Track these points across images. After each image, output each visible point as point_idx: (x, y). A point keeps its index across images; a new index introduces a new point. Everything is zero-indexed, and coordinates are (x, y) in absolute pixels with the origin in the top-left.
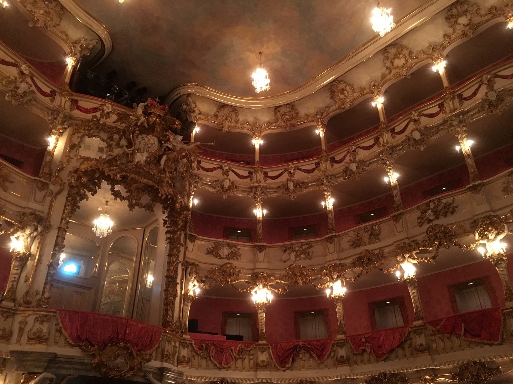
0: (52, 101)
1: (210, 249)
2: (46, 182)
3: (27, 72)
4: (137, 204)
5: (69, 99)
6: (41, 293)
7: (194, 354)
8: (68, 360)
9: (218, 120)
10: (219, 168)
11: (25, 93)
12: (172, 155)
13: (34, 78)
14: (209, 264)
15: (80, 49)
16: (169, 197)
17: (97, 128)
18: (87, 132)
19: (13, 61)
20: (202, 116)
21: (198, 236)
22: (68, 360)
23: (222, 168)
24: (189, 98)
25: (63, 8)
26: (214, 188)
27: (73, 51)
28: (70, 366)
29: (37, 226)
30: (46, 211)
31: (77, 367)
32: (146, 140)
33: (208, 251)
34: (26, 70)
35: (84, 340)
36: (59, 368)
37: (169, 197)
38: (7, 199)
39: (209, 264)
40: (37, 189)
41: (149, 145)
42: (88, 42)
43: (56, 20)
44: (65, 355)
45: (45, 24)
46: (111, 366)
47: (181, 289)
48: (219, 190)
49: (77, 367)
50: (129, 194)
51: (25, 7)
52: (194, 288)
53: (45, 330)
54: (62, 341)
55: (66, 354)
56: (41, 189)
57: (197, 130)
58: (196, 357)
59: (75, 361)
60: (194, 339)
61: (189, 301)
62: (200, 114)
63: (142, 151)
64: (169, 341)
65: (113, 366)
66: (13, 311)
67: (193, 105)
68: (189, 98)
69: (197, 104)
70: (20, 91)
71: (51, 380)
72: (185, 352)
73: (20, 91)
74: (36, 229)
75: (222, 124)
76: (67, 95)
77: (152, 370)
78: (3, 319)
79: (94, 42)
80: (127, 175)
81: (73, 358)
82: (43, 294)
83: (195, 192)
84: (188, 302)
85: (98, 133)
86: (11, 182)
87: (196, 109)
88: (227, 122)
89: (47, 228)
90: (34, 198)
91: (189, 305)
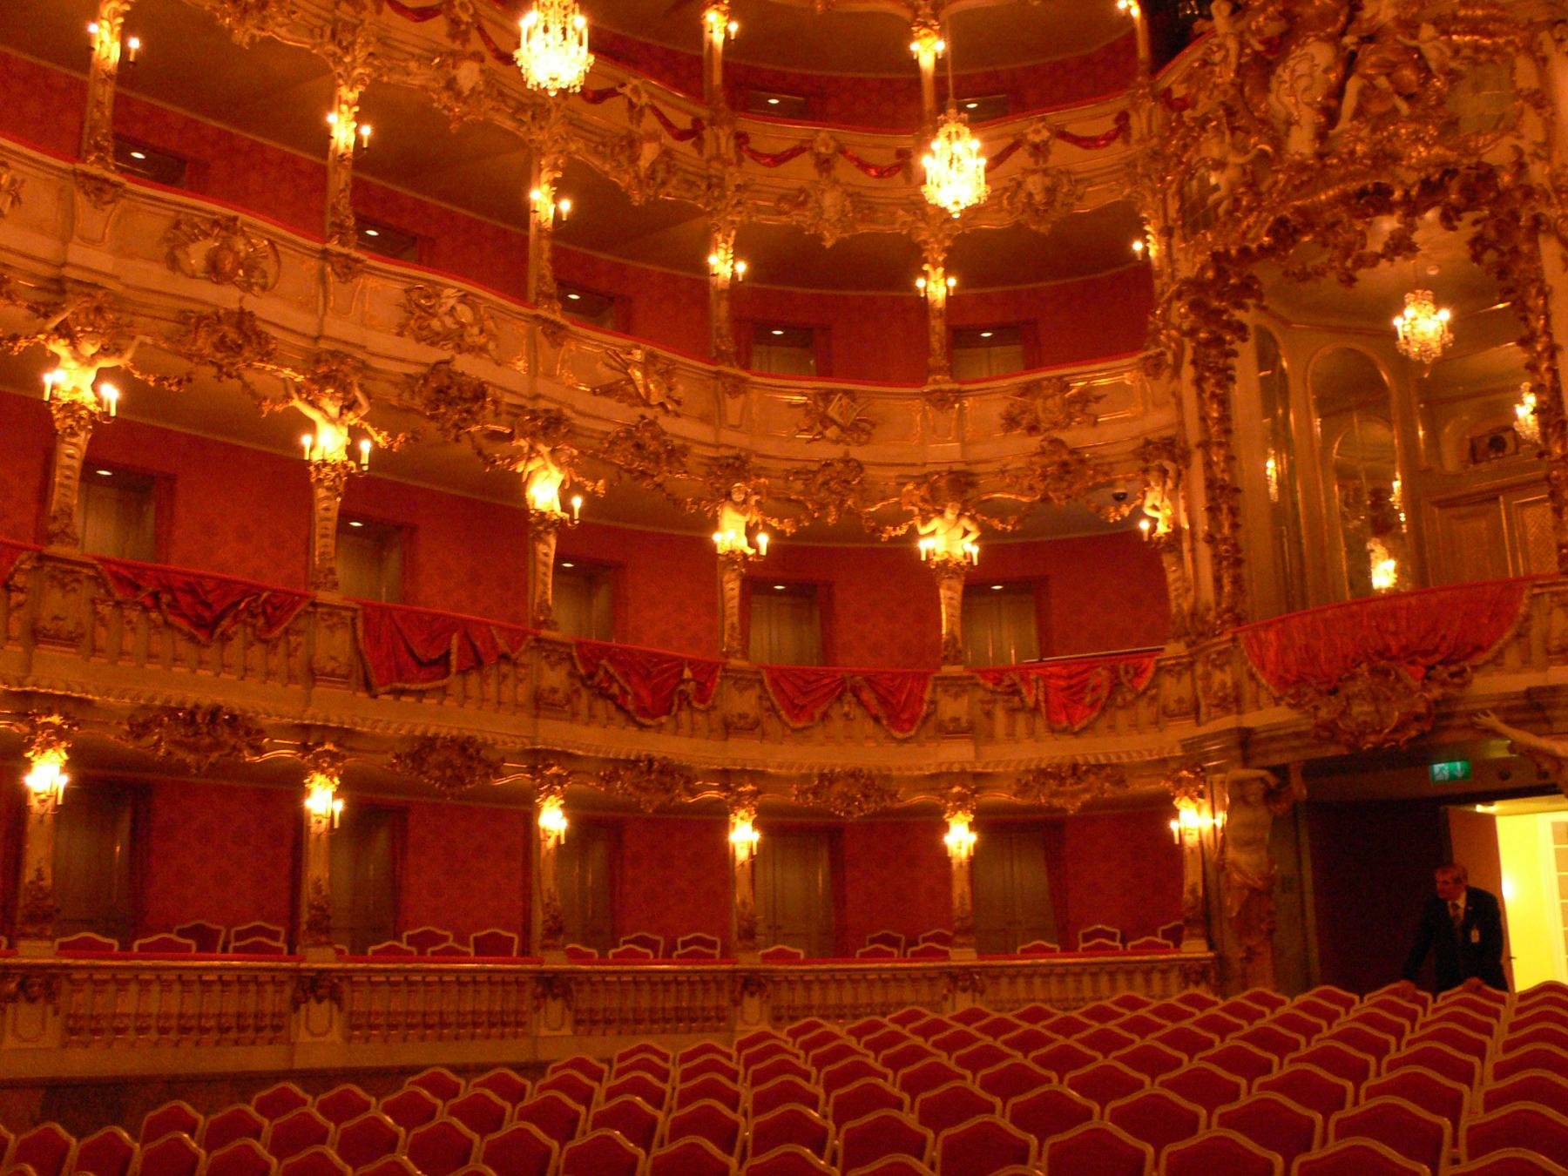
0: (1127, 142)
4: (1360, 262)
6: (1213, 604)
12: (1370, 59)
13: (1072, 129)
19: (1011, 141)
22: (1274, 736)
32: (1286, 76)
41: (1303, 83)
49: (1295, 743)
53: (1229, 683)
54: (1263, 696)
59: (1282, 732)
70: (1039, 198)
71: (1262, 779)
74: (1165, 473)
81: (1279, 727)
82: (1218, 604)
86: (1098, 399)
89: (1183, 458)
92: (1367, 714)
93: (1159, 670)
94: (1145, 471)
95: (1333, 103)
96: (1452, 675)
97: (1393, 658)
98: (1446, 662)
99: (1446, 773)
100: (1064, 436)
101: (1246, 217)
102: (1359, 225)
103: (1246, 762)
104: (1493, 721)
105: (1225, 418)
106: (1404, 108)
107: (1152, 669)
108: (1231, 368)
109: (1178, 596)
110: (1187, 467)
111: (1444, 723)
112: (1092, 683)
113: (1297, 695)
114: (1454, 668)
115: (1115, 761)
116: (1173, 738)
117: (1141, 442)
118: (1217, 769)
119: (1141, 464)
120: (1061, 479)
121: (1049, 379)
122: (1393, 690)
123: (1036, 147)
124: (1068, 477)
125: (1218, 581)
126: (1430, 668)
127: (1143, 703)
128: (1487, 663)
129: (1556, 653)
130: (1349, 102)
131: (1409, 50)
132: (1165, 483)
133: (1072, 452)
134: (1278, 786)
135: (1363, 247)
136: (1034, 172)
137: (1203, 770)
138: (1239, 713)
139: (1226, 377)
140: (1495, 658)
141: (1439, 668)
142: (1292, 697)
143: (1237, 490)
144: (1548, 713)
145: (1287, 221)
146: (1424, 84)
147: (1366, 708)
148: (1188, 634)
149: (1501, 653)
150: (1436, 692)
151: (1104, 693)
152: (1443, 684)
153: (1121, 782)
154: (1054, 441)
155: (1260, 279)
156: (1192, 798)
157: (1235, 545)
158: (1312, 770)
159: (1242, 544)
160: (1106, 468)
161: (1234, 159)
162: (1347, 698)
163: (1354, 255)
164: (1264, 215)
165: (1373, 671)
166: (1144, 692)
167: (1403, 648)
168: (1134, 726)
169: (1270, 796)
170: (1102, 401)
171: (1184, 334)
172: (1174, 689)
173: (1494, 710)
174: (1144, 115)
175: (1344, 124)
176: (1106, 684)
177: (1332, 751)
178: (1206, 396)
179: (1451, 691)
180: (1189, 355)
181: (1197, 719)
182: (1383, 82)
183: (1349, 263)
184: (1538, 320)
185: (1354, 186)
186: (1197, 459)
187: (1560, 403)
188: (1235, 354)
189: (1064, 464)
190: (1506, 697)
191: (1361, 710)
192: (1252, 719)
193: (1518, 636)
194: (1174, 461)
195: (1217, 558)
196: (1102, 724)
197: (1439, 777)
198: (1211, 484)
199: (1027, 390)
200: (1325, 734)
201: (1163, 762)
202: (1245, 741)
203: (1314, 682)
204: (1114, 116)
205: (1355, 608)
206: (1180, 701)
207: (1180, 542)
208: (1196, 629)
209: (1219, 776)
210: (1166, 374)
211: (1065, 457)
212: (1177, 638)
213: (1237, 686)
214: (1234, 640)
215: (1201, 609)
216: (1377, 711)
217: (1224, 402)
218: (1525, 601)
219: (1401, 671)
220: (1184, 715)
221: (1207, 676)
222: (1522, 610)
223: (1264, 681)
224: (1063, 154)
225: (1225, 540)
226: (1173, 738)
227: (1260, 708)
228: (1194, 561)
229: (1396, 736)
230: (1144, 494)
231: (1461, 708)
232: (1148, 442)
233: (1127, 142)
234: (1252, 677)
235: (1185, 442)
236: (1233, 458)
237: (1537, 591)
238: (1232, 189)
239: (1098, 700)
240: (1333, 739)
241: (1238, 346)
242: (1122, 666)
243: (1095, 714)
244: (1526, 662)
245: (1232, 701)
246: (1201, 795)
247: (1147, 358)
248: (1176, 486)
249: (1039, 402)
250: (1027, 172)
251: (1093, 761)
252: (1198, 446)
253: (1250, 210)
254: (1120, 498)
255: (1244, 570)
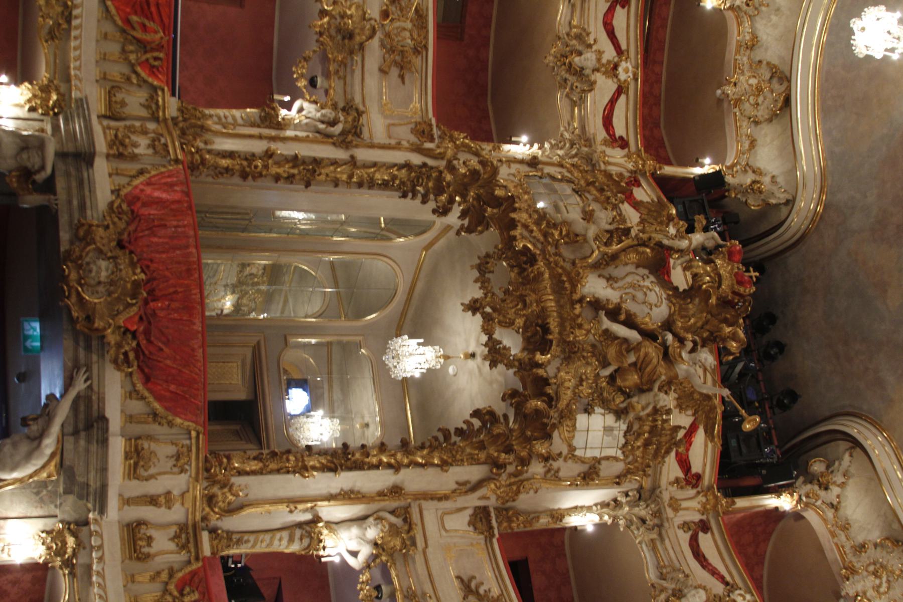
0: (605, 143)
1: (477, 587)
2: (436, 136)
3: (622, 76)
4: (487, 318)
5: (631, 172)
6: (209, 147)
7: (164, 576)
8: (86, 182)
9: (854, 560)
10: (727, 584)
11: (580, 73)
12: (651, 350)
13: (623, 98)
14: (432, 582)
15: (749, 181)
16: (550, 390)
17: (601, 190)
18: (582, 182)
19: (624, 47)
20: (830, 514)
21: (495, 541)
22: (84, 186)
23: (730, 591)
24: (847, 457)
25: (787, 102)
26: (662, 577)
27: (735, 169)
28: (75, 191)
29: (339, 122)
30: (376, 141)
31: (75, 202)
32: (647, 283)
33: (470, 580)
34: (626, 71)
35: (133, 211)
36: (68, 174)
37: (550, 390)
38: (367, 75)
39: (432, 582)
40: (413, 126)
41: (640, 295)
42: (774, 188)
43: (762, 113)
44: (95, 183)
45: (738, 102)
46: (88, 259)
47: (331, 498)
48: (663, 589)
49: (75, 202)
50: (501, 295)
51: (738, 52)
52: (345, 545)
53: (136, 151)
54: (123, 180)
55: (97, 186)
56: (413, 131)
57: (785, 502)
58: (157, 587)
59: (87, 193)
60: (204, 566)
61: (306, 542)
62: (835, 507)
63: (616, 285)
64: (178, 457)
65: (88, 264)
66: (161, 114)
67: (840, 479)
68: (847, 457)
69: (851, 481)
70: (577, 60)
71: (43, 168)
72: (162, 544)
73: (577, 60)
74: (333, 123)
75: (853, 571)
76: (636, 162)
77: (95, 388)
78: (143, 101)
79: (782, 197)
80: (536, 261)
81: (92, 191)
82: (209, 152)
83: (615, 524)
84: (301, 539)
85: (596, 200)
86: (402, 77)
87: (835, 490)
88: (871, 581)
90: (394, 125)
91: (295, 548)
92: (98, 272)
93: (155, 89)
94: (335, 107)
95: (622, 317)
96: (126, 354)
97: (146, 302)
98: (138, 350)
99: (31, 332)
100: (375, 42)
101: (540, 230)
102: (520, 322)
103: (61, 155)
104: (80, 385)
105: (371, 184)
106: (607, 372)
107: (155, 83)
108: (414, 197)
109: (219, 118)
110: (334, 144)
111: (82, 343)
112: (150, 24)
113: (120, 213)
114: (132, 355)
115: (74, 33)
116: (89, 90)
117: (361, 107)
118: (56, 128)
119: (341, 104)
120: (339, 30)
121: (426, 38)
122: (118, 299)
123: (616, 67)
124: (339, 37)
125: (231, 155)
126: (134, 335)
127: (126, 70)
128: (134, 385)
129: (136, 446)
130: (621, 331)
131: (651, 382)
132: (323, 122)
133: (362, 46)
134: (34, 182)
135: (500, 323)
136: (599, 60)
137: (56, 114)
138: (108, 156)
139: (406, 191)
140: (137, 392)
141: (134, 344)
142: (120, 206)
143: (308, 185)
144: (83, 434)
145: (532, 265)
146: (621, 390)
147: (104, 274)
148: (185, 120)
149: (143, 398)
150: (112, 338)
151: (139, 34)
152: (119, 345)
153: (51, 36)
154: (374, 31)
155: (486, 233)
156: (29, 101)
157: (261, 175)
158: (47, 218)
159: (260, 182)
160: (341, 73)
161: (592, 232)
162: (115, 258)
163: (495, 315)
164: (539, 246)
165: (136, 284)
166: (135, 72)
167: (154, 314)
168: (104, 57)
169: (26, 174)
170: (399, 80)
171: (449, 162)
172: (134, 101)
173: (90, 387)
174: (622, 161)
175: (607, 323)
176: (148, 37)
177: (65, 236)
178: (394, 171)
179: (112, 352)
180: (430, 162)
181: (105, 117)
182: (632, 358)
183: (488, 310)
184: (422, 457)
185: (553, 324)
186: (341, 154)
187: (350, 469)
188: (424, 202)
189: (350, 36)
190: (101, 400)
191: (103, 269)
192: (101, 167)
193: (155, 415)
194: (343, 133)
195: (250, 158)
196: (109, 27)
197: (26, 325)
198: (317, 162)
199: (420, 15)
200: (81, 233)
201: (68, 79)
202: (83, 158)
203: (131, 228)
204: (625, 136)
205: (196, 276)
206: (123, 104)
207: (269, 127)
208: (190, 127)
209: (49, 128)
210: (413, 139)
211: (358, 39)
212: (180, 110)
213: (134, 158)
214: (177, 161)
215: (208, 136)
216: (99, 283)
217: (385, 185)
218: (186, 423)
219: (135, 309)
220: (110, 104)
221: (144, 132)
222: (178, 421)
223: (136, 182)
224: (605, 87)
225: (266, 167)
226: (89, 90)
227: (110, 175)
228: (251, 136)
229: (74, 299)
230: (315, 102)
231: (95, 358)
232: (360, 114)
233: (605, 143)
234: (141, 172)
235: (357, 146)
236: (336, 185)
237: (194, 434)
238: (565, 223)
239: (133, 28)
240: (75, 238)
241: (432, 205)
242: (161, 55)
243: (120, 23)
244: (130, 419)
245: (120, 151)
246: (32, 109)
247: (431, 125)
248: (318, 132)
249: (409, 25)
250: (600, 53)
251: (75, 12)
252: (352, 157)
253: (545, 235)
254: (313, 83)
255: (237, 180)
